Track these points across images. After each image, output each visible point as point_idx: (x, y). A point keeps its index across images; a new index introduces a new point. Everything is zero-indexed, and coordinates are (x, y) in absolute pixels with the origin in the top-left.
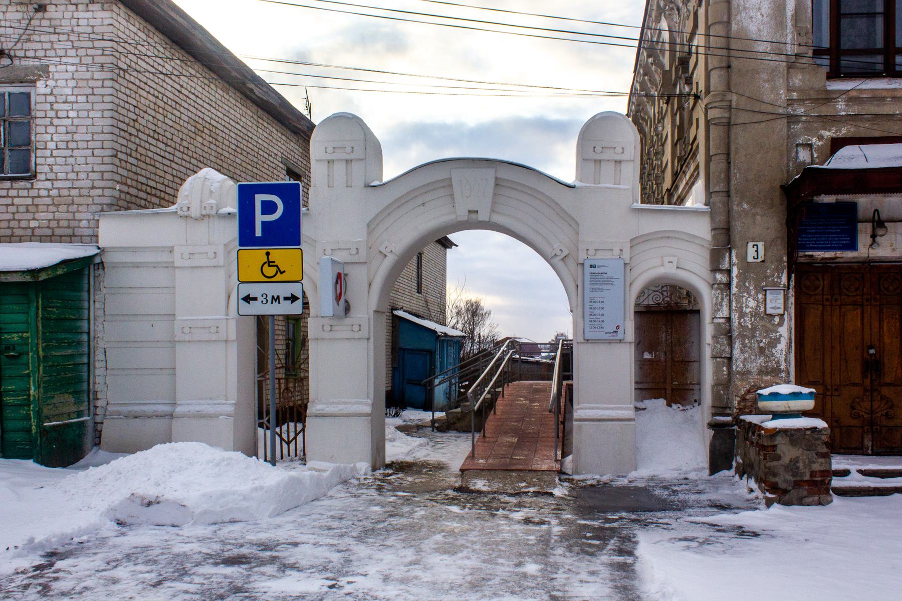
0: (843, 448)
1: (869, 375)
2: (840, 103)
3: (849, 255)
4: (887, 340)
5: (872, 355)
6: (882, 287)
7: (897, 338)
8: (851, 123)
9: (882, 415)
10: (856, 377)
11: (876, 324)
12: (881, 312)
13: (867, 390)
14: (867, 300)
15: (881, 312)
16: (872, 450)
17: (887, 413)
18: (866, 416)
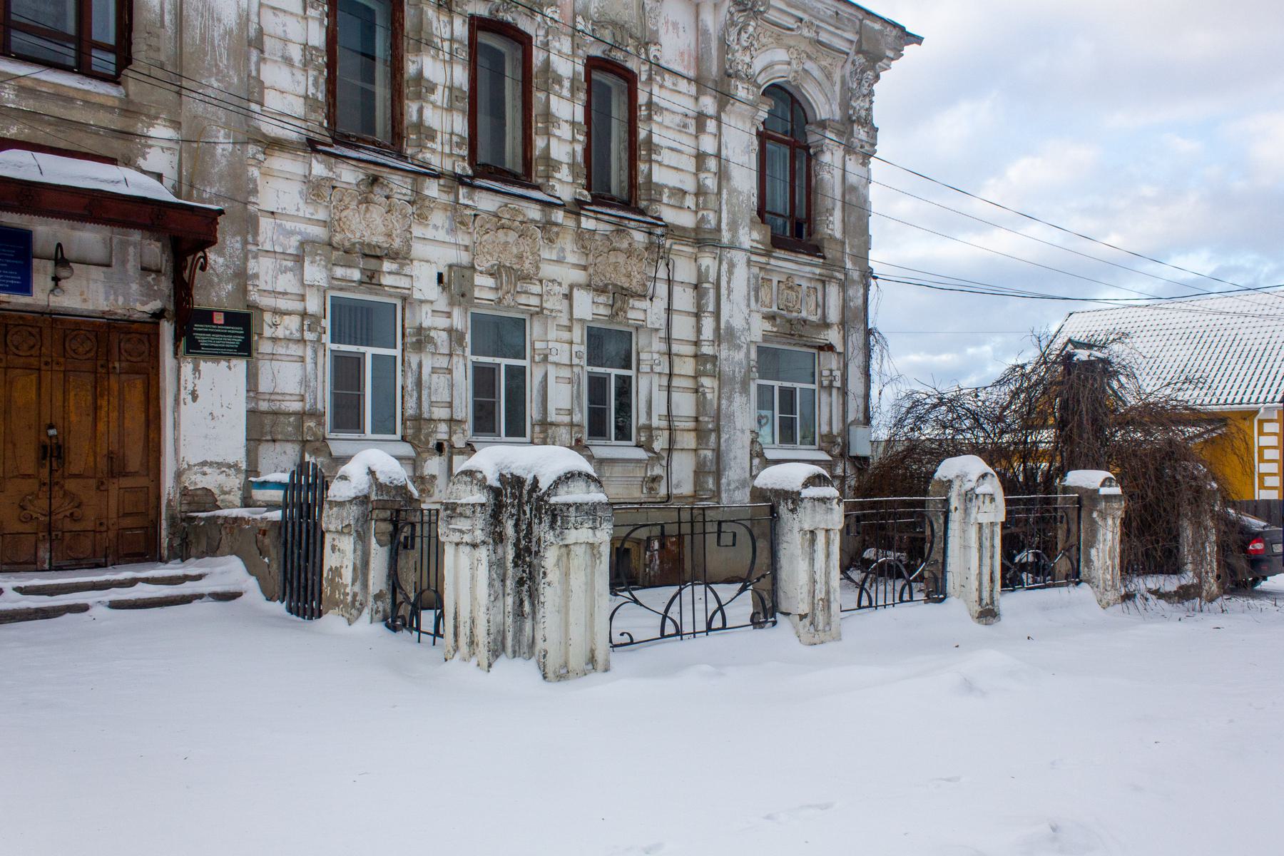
0: (6, 564)
1: (48, 464)
2: (7, 91)
3: (19, 300)
4: (73, 418)
5: (51, 437)
6: (67, 347)
7: (88, 415)
8: (25, 121)
9: (65, 516)
10: (29, 465)
11: (59, 396)
12: (66, 381)
13: (44, 484)
14: (46, 363)
15: (66, 381)
16: (50, 564)
17: (72, 514)
18: (42, 518)
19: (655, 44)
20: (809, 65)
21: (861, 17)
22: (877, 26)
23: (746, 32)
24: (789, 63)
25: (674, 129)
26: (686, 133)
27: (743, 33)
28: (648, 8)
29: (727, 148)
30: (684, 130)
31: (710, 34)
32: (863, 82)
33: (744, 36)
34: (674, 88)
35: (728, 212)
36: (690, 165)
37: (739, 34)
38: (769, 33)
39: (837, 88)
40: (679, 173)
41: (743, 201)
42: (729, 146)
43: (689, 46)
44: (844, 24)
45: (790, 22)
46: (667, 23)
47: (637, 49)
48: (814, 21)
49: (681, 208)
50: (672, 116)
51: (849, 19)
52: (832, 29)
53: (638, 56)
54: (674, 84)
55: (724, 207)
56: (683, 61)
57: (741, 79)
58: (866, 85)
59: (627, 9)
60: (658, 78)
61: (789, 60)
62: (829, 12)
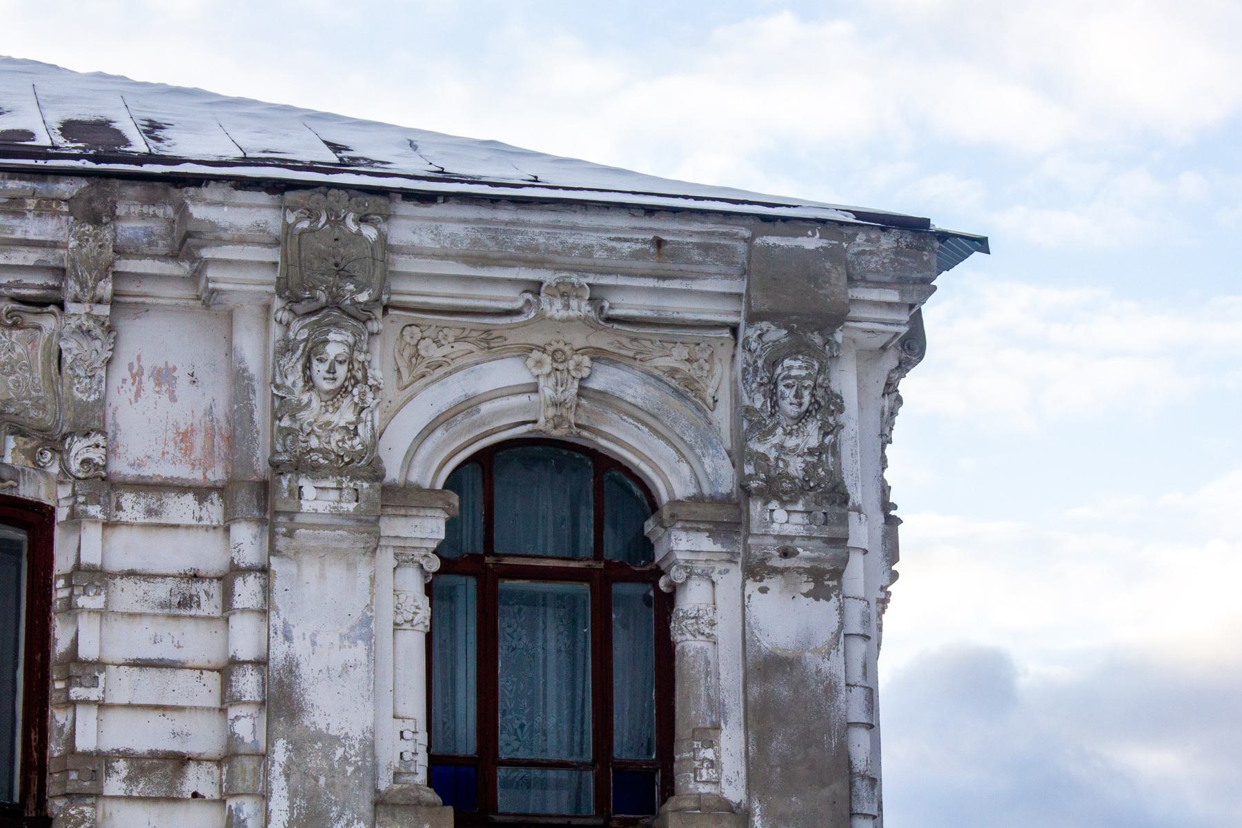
19: (87, 435)
20: (603, 379)
21: (746, 233)
22: (811, 242)
23: (321, 360)
24: (535, 389)
25: (155, 615)
26: (191, 617)
27: (315, 363)
28: (68, 358)
29: (288, 637)
30: (183, 612)
31: (250, 379)
32: (781, 388)
33: (319, 369)
34: (154, 520)
35: (293, 794)
36: (206, 691)
37: (307, 367)
38: (451, 335)
39: (722, 416)
40: (168, 714)
41: (345, 760)
42: (296, 633)
43: (209, 412)
44: (690, 262)
45: (510, 298)
46: (137, 376)
47: (33, 456)
48: (574, 278)
49: (172, 799)
50: (144, 586)
51: (706, 248)
52: (651, 283)
53: (40, 468)
54: (150, 512)
55: (279, 787)
56: (188, 451)
57: (314, 470)
58: (790, 393)
59: (13, 372)
60: (94, 510)
61: (530, 380)
62: (626, 247)
